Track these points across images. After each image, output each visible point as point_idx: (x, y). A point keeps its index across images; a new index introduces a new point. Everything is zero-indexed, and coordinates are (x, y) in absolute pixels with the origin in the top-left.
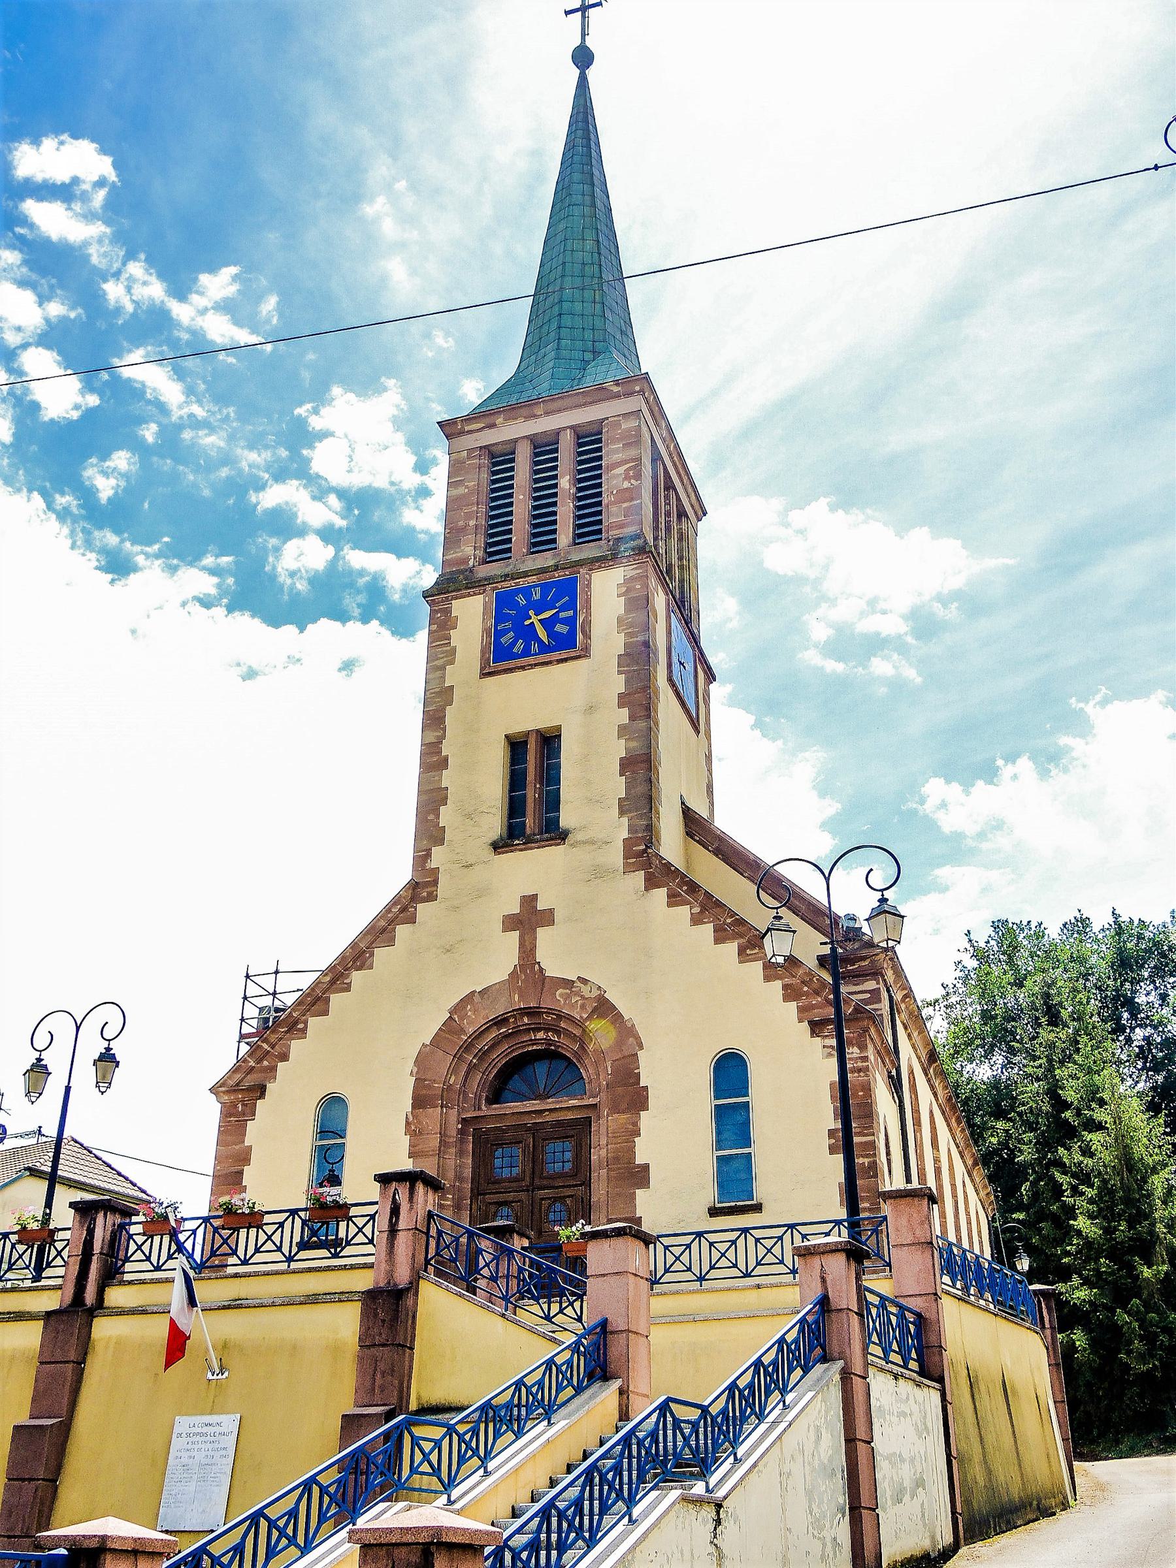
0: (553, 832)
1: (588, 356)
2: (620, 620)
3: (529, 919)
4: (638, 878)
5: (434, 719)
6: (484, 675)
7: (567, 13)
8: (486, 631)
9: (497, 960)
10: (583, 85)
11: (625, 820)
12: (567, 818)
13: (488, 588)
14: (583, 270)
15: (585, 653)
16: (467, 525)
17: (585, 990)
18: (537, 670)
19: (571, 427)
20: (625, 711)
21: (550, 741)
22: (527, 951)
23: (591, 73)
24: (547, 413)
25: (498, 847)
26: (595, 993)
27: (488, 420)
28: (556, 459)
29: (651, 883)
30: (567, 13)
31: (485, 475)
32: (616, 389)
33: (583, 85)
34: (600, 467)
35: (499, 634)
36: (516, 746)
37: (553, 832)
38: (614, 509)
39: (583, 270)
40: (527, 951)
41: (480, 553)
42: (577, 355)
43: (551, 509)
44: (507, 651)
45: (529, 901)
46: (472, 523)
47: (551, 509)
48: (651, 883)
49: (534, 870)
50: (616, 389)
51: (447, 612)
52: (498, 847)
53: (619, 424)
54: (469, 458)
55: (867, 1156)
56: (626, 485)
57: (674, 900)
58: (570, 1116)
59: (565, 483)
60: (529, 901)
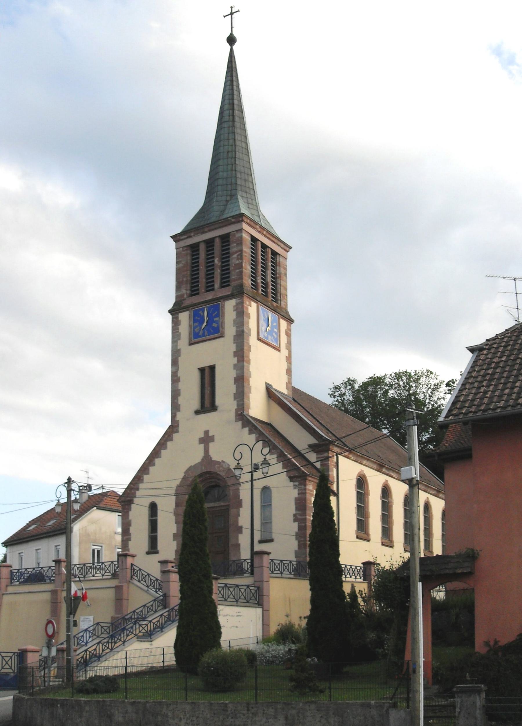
0: (213, 408)
1: (228, 198)
2: (234, 321)
3: (207, 439)
4: (240, 423)
5: (175, 363)
6: (191, 344)
7: (224, 17)
8: (190, 326)
9: (196, 456)
10: (232, 51)
11: (236, 401)
12: (218, 402)
13: (190, 308)
14: (228, 155)
15: (222, 336)
16: (183, 280)
17: (224, 465)
18: (207, 343)
19: (219, 236)
20: (236, 358)
21: (212, 368)
22: (206, 451)
23: (234, 47)
24: (210, 231)
25: (197, 412)
26: (227, 466)
27: (188, 235)
28: (213, 249)
29: (243, 426)
30: (224, 17)
31: (189, 258)
32: (233, 220)
33: (232, 51)
34: (228, 253)
35: (195, 328)
36: (202, 370)
37: (213, 408)
38: (233, 273)
39: (228, 155)
40: (206, 451)
41: (188, 292)
42: (224, 198)
43: (227, 247)
44: (196, 338)
45: (206, 432)
46: (185, 279)
47: (227, 247)
48: (243, 426)
49: (207, 421)
50: (233, 220)
51: (177, 318)
52: (197, 412)
53: (234, 235)
54: (183, 251)
55: (303, 523)
56: (237, 262)
57: (250, 432)
58: (222, 508)
59: (216, 261)
60: (206, 432)
